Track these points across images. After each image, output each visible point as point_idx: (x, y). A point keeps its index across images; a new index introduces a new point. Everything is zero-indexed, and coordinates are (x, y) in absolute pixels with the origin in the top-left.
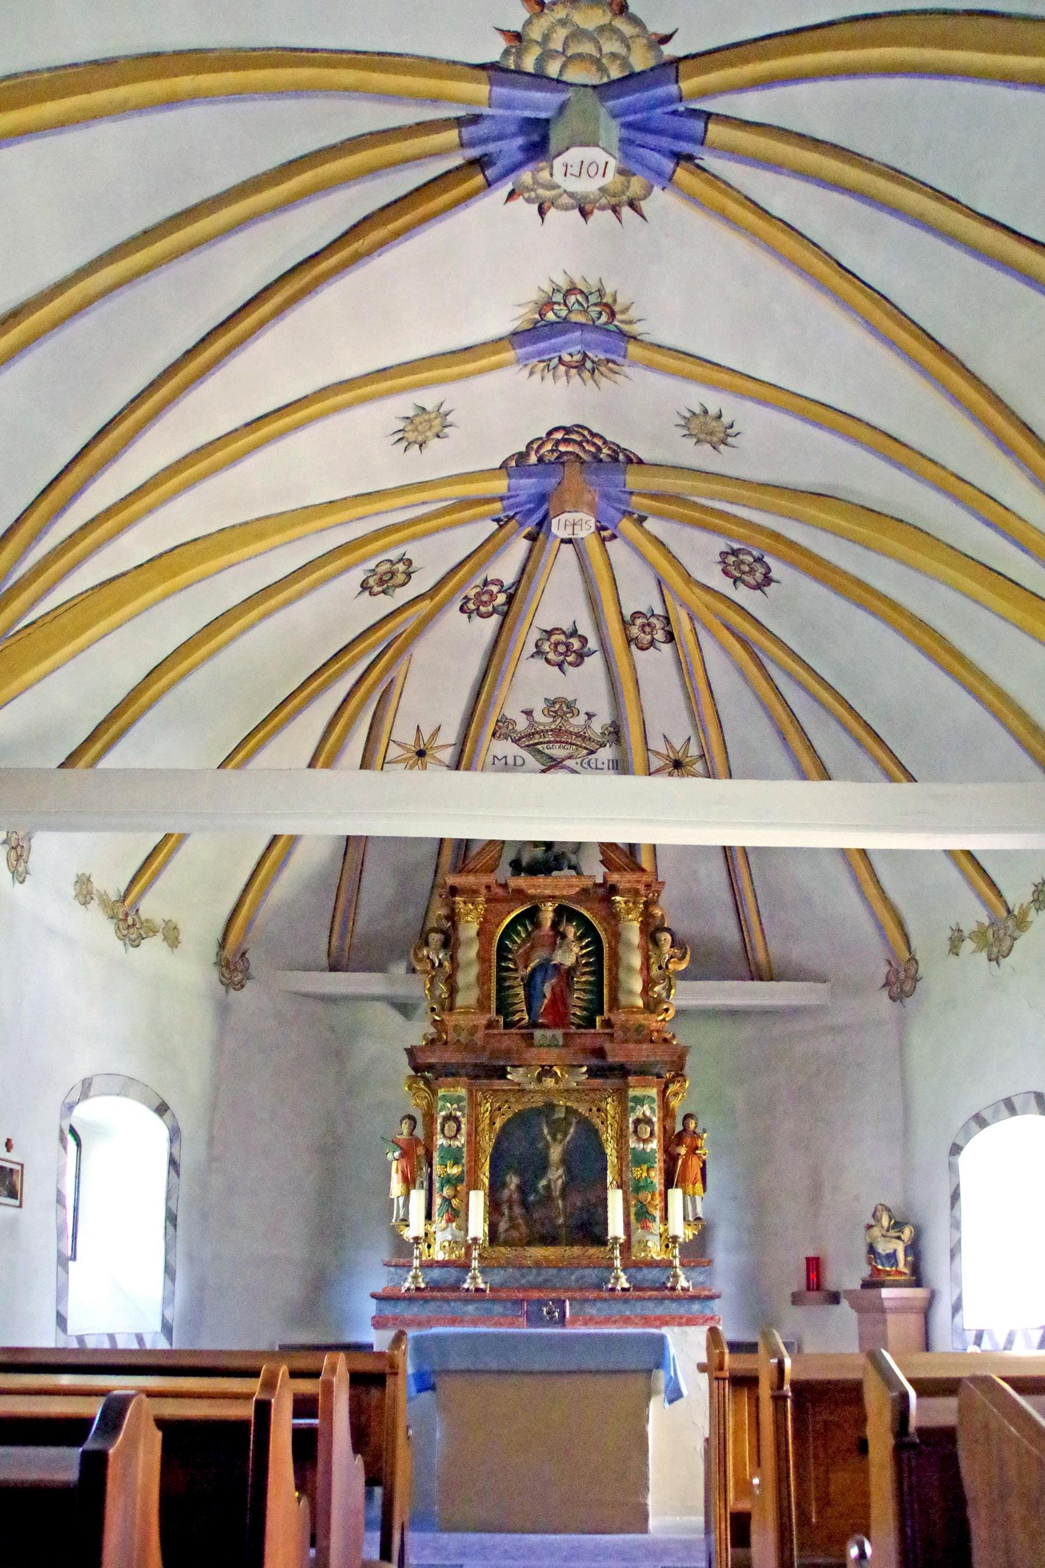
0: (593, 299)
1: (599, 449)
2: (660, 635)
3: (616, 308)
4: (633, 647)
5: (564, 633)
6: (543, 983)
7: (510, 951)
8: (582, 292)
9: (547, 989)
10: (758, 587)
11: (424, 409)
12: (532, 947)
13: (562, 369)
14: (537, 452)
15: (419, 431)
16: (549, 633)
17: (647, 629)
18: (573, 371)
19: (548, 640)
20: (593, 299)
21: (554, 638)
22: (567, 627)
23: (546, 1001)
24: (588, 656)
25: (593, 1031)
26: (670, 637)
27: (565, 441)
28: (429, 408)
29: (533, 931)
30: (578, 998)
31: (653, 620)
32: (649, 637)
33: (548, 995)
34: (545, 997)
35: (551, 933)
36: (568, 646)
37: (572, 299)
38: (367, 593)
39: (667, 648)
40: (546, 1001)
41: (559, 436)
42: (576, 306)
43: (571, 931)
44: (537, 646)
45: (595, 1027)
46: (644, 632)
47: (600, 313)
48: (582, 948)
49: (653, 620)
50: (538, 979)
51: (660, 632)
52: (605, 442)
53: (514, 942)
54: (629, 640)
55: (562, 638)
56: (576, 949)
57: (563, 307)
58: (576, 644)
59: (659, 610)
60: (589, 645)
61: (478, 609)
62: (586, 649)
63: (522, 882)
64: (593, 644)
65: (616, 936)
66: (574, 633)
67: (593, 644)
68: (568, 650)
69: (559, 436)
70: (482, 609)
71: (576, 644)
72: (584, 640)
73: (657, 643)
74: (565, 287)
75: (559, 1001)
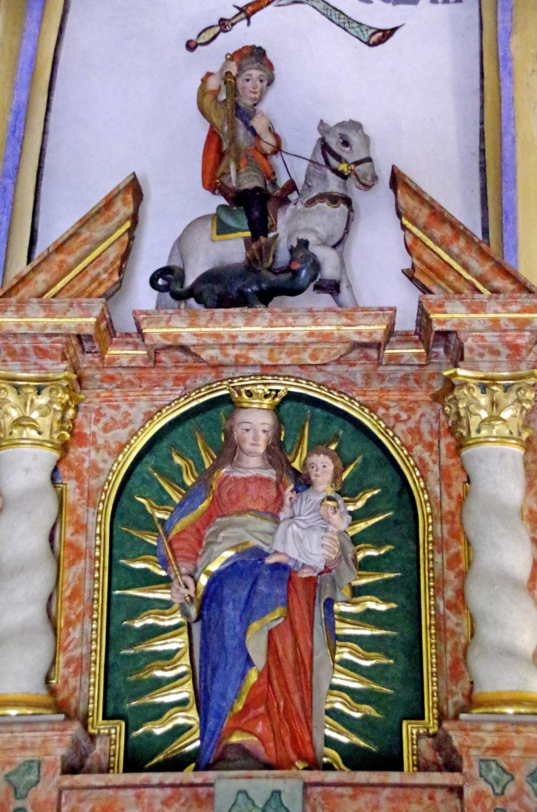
6: (246, 624)
7: (148, 524)
9: (257, 646)
12: (208, 518)
23: (253, 676)
25: (394, 777)
29: (216, 466)
30: (346, 663)
33: (259, 659)
34: (249, 662)
35: (270, 474)
40: (253, 676)
43: (322, 468)
45: (399, 767)
48: (356, 517)
50: (231, 612)
53: (163, 501)
56: (340, 522)
63: (188, 327)
65: (460, 479)
75: (292, 671)
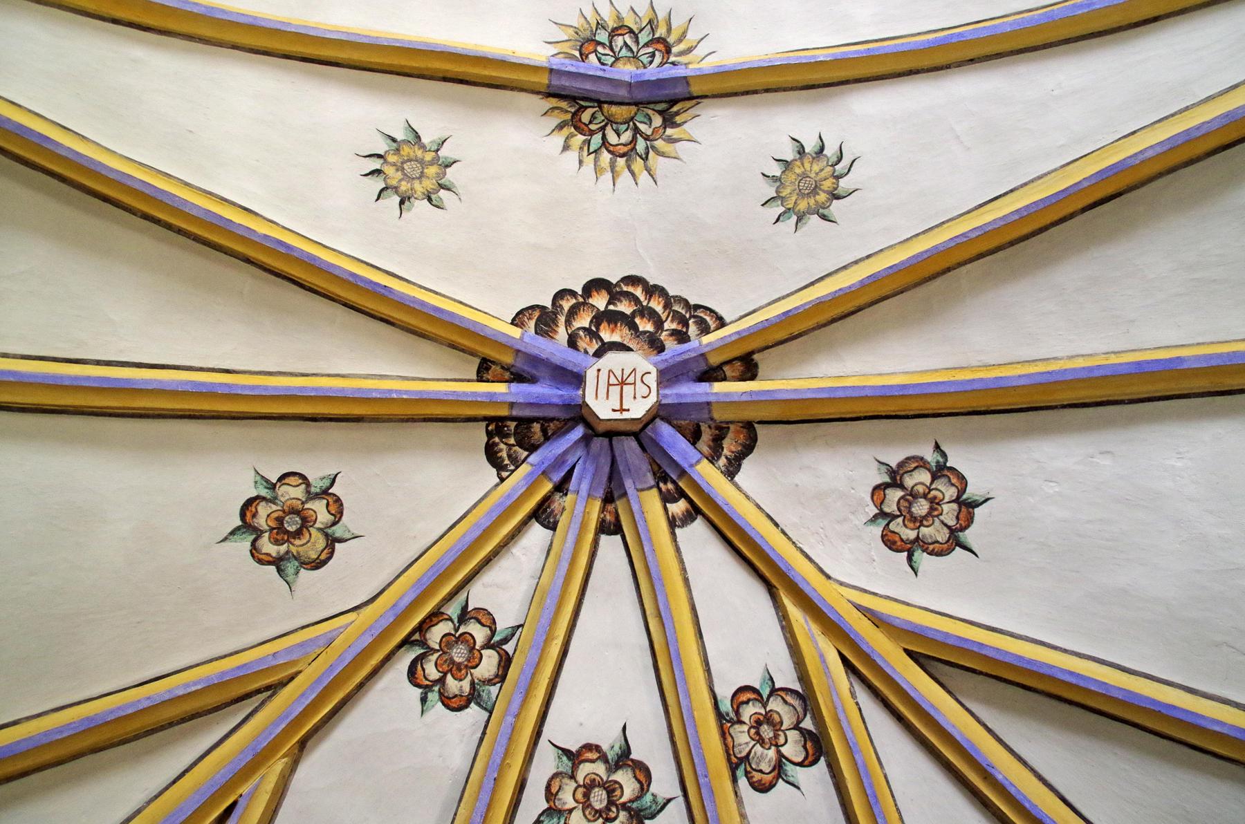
0: (644, 38)
1: (659, 324)
2: (793, 748)
3: (671, 40)
4: (743, 782)
5: (604, 758)
8: (631, 31)
10: (955, 541)
11: (418, 137)
13: (606, 157)
14: (568, 323)
15: (408, 172)
16: (575, 757)
17: (767, 732)
18: (621, 162)
19: (573, 777)
20: (644, 38)
21: (585, 770)
22: (609, 741)
24: (652, 817)
26: (817, 747)
27: (611, 318)
28: (425, 140)
31: (775, 705)
32: (772, 753)
36: (611, 789)
37: (619, 41)
38: (245, 544)
39: (815, 778)
41: (600, 301)
42: (624, 52)
44: (550, 795)
46: (761, 741)
47: (653, 55)
49: (775, 705)
51: (793, 735)
52: (668, 301)
54: (737, 763)
55: (600, 769)
57: (608, 51)
58: (626, 781)
59: (786, 678)
60: (653, 788)
61: (442, 681)
62: (648, 798)
64: (664, 783)
66: (624, 759)
67: (664, 783)
68: (611, 803)
69: (600, 301)
70: (452, 684)
71: (626, 781)
72: (643, 773)
73: (789, 768)
74: (611, 24)
